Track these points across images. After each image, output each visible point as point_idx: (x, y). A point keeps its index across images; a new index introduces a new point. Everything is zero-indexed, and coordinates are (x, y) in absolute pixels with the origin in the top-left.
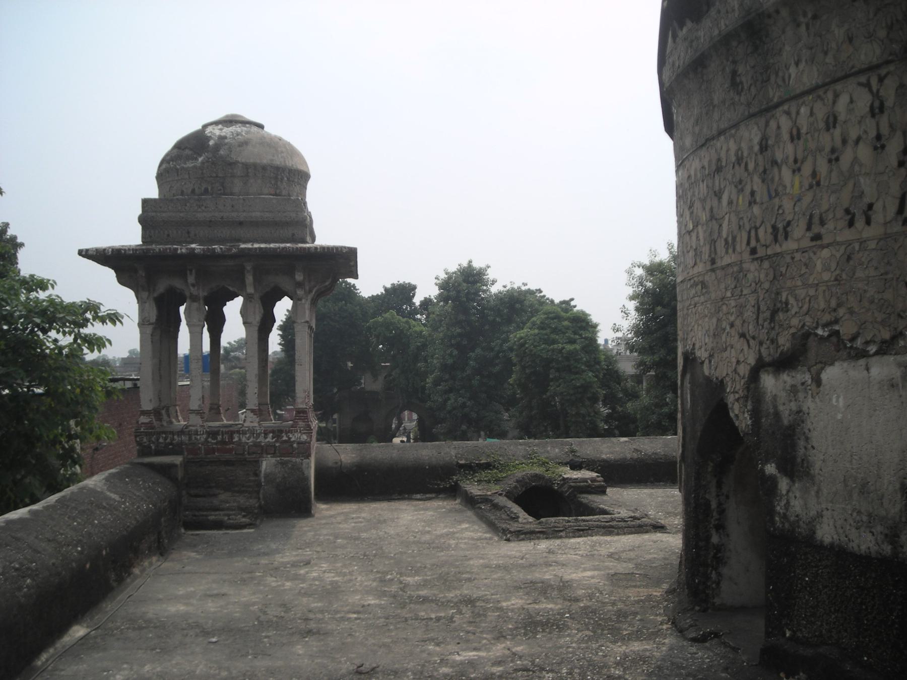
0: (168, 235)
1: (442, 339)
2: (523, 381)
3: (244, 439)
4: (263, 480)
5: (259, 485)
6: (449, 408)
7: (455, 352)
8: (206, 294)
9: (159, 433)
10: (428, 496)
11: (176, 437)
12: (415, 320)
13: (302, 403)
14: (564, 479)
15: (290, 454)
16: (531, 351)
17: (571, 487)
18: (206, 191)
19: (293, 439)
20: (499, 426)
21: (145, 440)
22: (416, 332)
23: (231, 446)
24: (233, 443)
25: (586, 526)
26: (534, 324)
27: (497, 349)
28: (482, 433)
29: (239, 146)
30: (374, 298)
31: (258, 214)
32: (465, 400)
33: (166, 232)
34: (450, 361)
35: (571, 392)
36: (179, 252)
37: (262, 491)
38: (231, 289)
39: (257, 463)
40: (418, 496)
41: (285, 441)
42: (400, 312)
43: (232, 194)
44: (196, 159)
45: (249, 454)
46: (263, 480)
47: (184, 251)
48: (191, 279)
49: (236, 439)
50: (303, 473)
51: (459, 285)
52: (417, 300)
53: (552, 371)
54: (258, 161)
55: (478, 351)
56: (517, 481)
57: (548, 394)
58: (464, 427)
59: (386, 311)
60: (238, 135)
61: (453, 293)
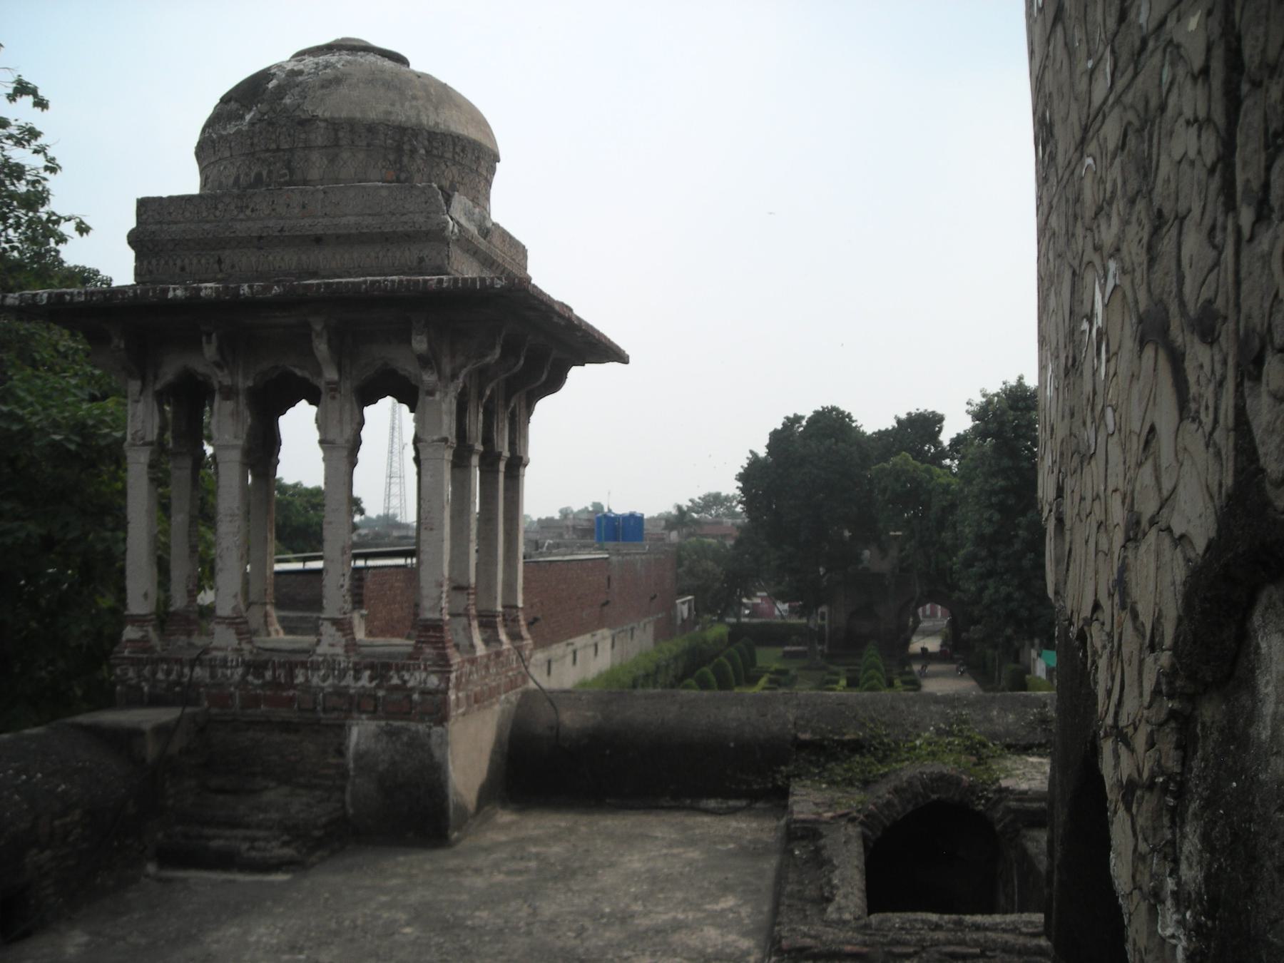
0: (183, 269)
3: (315, 681)
4: (351, 765)
5: (344, 775)
7: (997, 517)
8: (250, 383)
9: (156, 662)
10: (732, 803)
11: (186, 670)
12: (942, 467)
13: (433, 609)
14: (1001, 790)
15: (406, 715)
17: (1009, 810)
18: (259, 177)
19: (411, 684)
21: (131, 674)
23: (291, 693)
24: (295, 687)
25: (976, 943)
28: (1037, 641)
29: (322, 87)
30: (881, 435)
31: (352, 219)
33: (179, 262)
34: (988, 530)
36: (171, 295)
37: (349, 788)
38: (299, 372)
39: (340, 729)
40: (712, 803)
41: (396, 688)
42: (919, 455)
43: (305, 182)
44: (242, 117)
45: (325, 710)
46: (351, 765)
47: (179, 293)
48: (210, 351)
49: (300, 679)
50: (431, 756)
51: (1004, 413)
52: (946, 438)
54: (358, 115)
56: (896, 791)
59: (897, 453)
60: (326, 67)
61: (993, 426)
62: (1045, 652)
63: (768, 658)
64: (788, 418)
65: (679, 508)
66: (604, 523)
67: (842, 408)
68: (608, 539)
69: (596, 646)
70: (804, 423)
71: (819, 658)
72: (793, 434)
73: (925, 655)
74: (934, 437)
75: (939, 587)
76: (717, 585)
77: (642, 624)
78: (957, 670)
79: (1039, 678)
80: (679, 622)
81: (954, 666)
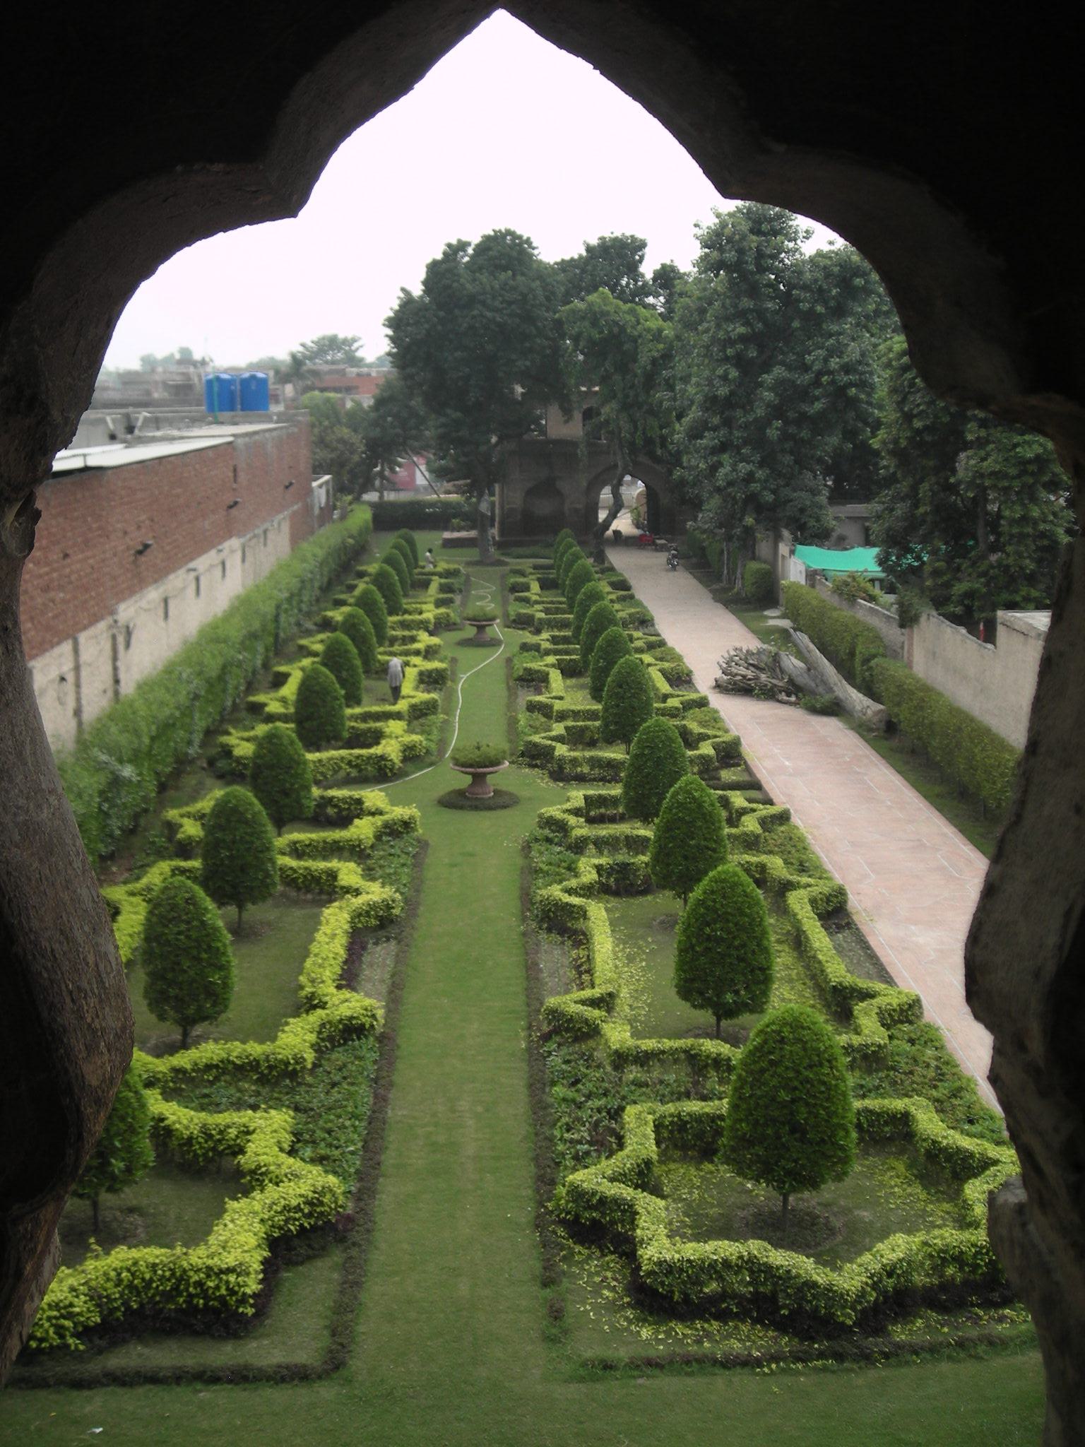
1: (707, 347)
2: (903, 443)
7: (734, 373)
12: (646, 306)
20: (818, 520)
22: (649, 330)
27: (816, 367)
28: (786, 533)
30: (565, 266)
32: (749, 467)
34: (723, 391)
35: (1013, 471)
52: (648, 269)
53: (972, 426)
55: (778, 371)
59: (596, 289)
61: (730, 256)
62: (799, 547)
64: (449, 245)
65: (294, 356)
66: (216, 389)
67: (519, 232)
68: (221, 410)
69: (223, 564)
70: (470, 251)
71: (492, 550)
74: (632, 268)
76: (356, 458)
77: (275, 524)
78: (669, 562)
79: (797, 584)
80: (317, 511)
81: (662, 558)
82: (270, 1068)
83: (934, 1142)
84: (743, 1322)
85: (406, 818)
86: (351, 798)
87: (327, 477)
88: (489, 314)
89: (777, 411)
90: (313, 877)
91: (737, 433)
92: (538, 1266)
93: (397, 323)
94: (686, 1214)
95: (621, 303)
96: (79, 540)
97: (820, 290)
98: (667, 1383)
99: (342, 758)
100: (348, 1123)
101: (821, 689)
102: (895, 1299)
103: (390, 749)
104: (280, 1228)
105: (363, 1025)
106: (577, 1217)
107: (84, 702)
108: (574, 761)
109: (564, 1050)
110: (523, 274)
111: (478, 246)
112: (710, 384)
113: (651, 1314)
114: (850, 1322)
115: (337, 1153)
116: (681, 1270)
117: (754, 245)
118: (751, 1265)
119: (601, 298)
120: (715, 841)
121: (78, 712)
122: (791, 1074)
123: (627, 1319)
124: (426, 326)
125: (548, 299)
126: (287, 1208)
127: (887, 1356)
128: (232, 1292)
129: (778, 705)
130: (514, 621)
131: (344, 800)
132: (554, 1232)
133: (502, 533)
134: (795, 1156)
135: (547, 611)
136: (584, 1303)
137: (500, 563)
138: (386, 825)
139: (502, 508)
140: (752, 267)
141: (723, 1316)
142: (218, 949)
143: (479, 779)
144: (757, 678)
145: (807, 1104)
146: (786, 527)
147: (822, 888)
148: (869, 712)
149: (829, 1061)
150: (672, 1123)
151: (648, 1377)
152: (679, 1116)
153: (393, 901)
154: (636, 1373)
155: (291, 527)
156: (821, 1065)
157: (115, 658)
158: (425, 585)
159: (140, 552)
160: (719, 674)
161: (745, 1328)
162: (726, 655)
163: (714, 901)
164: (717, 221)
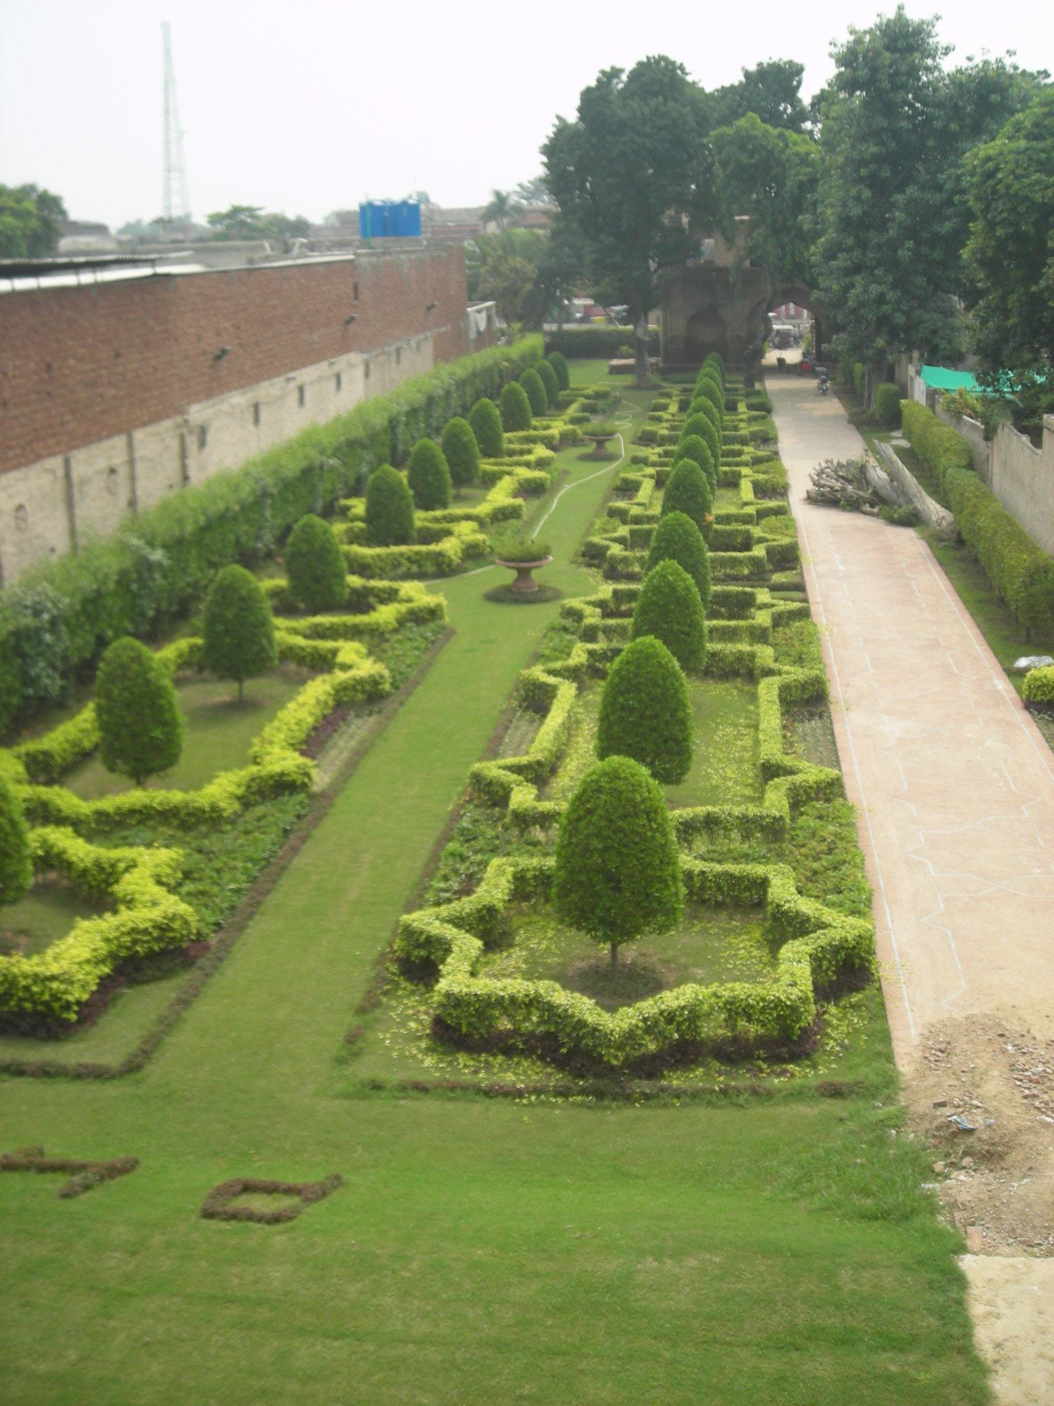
1: (841, 168)
2: (990, 253)
6: (851, 304)
7: (867, 193)
12: (800, 131)
16: (1009, 187)
20: (950, 342)
22: (797, 154)
26: (1018, 127)
27: (949, 186)
28: (916, 354)
34: (856, 212)
42: (773, 117)
51: (877, 54)
55: (911, 190)
57: (1042, 283)
58: (880, 342)
59: (743, 115)
61: (863, 73)
62: (927, 370)
63: (589, 377)
64: (603, 72)
65: (498, 195)
66: (369, 215)
67: (672, 58)
68: (374, 234)
69: (338, 377)
70: (624, 77)
72: (611, 92)
73: (782, 368)
74: (790, 93)
75: (795, 284)
76: (529, 286)
77: (413, 343)
80: (473, 335)
81: (813, 383)
82: (189, 815)
83: (778, 906)
84: (527, 1057)
85: (432, 605)
86: (391, 588)
87: (489, 303)
88: (639, 140)
89: (911, 232)
90: (320, 656)
91: (870, 255)
92: (358, 997)
93: (552, 150)
94: (525, 962)
95: (769, 127)
96: (138, 341)
97: (956, 108)
98: (429, 1106)
99: (402, 555)
100: (240, 865)
101: (901, 501)
102: (682, 1047)
103: (450, 547)
104: (128, 948)
105: (294, 782)
106: (409, 954)
107: (139, 493)
108: (625, 560)
109: (479, 811)
110: (675, 100)
111: (631, 72)
112: (844, 204)
113: (443, 1044)
114: (615, 1062)
115: (215, 889)
116: (469, 1004)
117: (887, 62)
118: (533, 1002)
119: (749, 122)
120: (690, 626)
121: (132, 503)
122: (603, 823)
123: (419, 1049)
124: (578, 152)
125: (699, 124)
126: (134, 931)
127: (647, 1097)
128: (55, 997)
129: (862, 516)
130: (640, 438)
131: (383, 590)
132: (387, 969)
133: (665, 361)
134: (608, 904)
135: (673, 428)
136: (386, 1031)
137: (656, 387)
138: (411, 612)
139: (665, 333)
140: (886, 85)
141: (509, 1052)
142: (161, 706)
143: (524, 573)
144: (843, 490)
145: (620, 854)
146: (919, 349)
147: (795, 674)
148: (944, 523)
149: (648, 814)
150: (535, 877)
151: (412, 1098)
152: (541, 870)
153: (382, 677)
154: (400, 1095)
155: (435, 348)
156: (636, 815)
157: (183, 456)
158: (562, 406)
159: (218, 358)
160: (810, 486)
161: (526, 1063)
162: (818, 468)
163: (628, 671)
164: (852, 38)
